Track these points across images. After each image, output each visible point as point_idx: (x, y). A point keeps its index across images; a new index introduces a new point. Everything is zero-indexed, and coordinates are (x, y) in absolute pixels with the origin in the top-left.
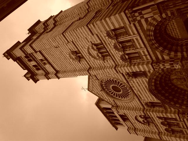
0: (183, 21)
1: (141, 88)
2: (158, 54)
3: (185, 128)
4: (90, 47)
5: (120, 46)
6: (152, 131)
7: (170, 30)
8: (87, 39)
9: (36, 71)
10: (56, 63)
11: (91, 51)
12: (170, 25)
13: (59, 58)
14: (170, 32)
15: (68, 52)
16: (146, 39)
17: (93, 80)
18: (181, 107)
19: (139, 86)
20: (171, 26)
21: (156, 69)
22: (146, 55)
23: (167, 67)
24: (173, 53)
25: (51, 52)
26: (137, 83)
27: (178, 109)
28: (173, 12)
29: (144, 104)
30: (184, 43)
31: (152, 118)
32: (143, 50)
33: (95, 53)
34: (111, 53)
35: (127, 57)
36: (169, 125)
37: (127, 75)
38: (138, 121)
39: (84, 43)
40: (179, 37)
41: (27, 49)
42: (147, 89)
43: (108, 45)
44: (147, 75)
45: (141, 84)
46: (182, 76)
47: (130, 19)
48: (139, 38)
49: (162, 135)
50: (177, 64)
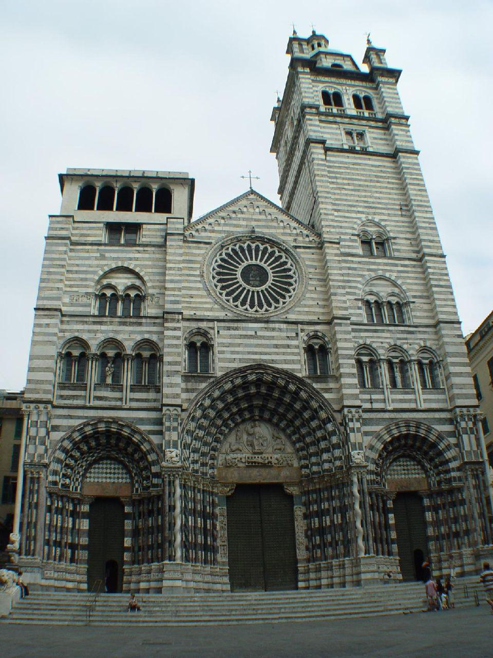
1: (268, 346)
4: (396, 290)
8: (420, 297)
9: (321, 87)
10: (354, 169)
11: (387, 286)
12: (416, 467)
13: (371, 192)
15: (388, 229)
16: (413, 418)
17: (295, 232)
19: (276, 346)
20: (415, 469)
23: (352, 435)
25: (388, 183)
26: (288, 346)
27: (190, 410)
29: (204, 325)
31: (140, 324)
32: (390, 401)
33: (382, 292)
34: (383, 331)
37: (313, 333)
38: (112, 271)
39: (411, 284)
41: (404, 133)
42: (265, 361)
43: (405, 336)
44: (317, 382)
45: (284, 354)
46: (270, 450)
47: (464, 410)
48: (413, 406)
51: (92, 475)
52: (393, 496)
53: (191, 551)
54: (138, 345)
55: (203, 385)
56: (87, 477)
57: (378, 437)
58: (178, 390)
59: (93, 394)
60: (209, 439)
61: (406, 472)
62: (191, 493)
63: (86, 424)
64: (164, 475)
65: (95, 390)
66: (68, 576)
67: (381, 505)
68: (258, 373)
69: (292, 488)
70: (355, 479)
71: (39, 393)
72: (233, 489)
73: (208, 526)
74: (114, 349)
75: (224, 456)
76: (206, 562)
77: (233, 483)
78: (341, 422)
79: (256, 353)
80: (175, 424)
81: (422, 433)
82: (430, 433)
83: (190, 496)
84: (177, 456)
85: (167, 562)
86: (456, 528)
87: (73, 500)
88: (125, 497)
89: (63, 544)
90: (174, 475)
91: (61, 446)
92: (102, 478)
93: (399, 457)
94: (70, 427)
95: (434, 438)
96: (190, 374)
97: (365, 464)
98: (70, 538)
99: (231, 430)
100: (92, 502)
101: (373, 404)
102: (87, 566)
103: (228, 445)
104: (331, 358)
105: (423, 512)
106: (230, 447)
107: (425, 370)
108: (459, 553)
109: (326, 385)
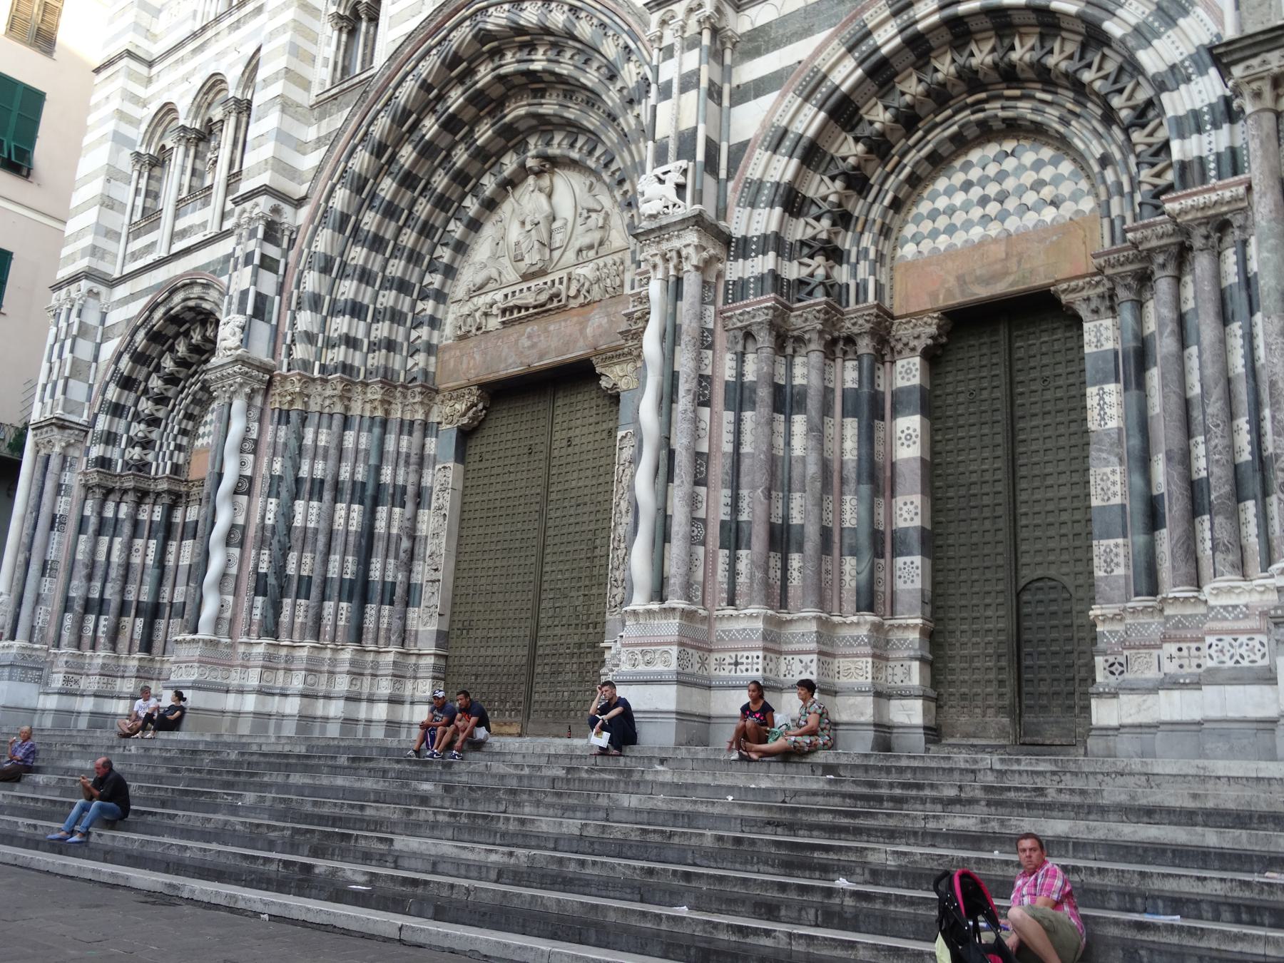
0: (1057, 282)
2: (799, 51)
3: (171, 243)
6: (160, 11)
7: (1001, 177)
12: (1047, 173)
14: (975, 174)
20: (1038, 185)
21: (664, 23)
23: (665, 109)
24: (782, 168)
27: (315, 197)
28: (1204, 178)
30: (854, 275)
36: (203, 136)
40: (917, 239)
46: (570, 256)
49: (131, 75)
50: (680, 188)
57: (812, 85)
63: (153, 307)
68: (475, 14)
69: (617, 369)
70: (655, 289)
71: (74, 261)
73: (381, 526)
87: (158, 494)
93: (961, 143)
96: (326, 95)
99: (475, 225)
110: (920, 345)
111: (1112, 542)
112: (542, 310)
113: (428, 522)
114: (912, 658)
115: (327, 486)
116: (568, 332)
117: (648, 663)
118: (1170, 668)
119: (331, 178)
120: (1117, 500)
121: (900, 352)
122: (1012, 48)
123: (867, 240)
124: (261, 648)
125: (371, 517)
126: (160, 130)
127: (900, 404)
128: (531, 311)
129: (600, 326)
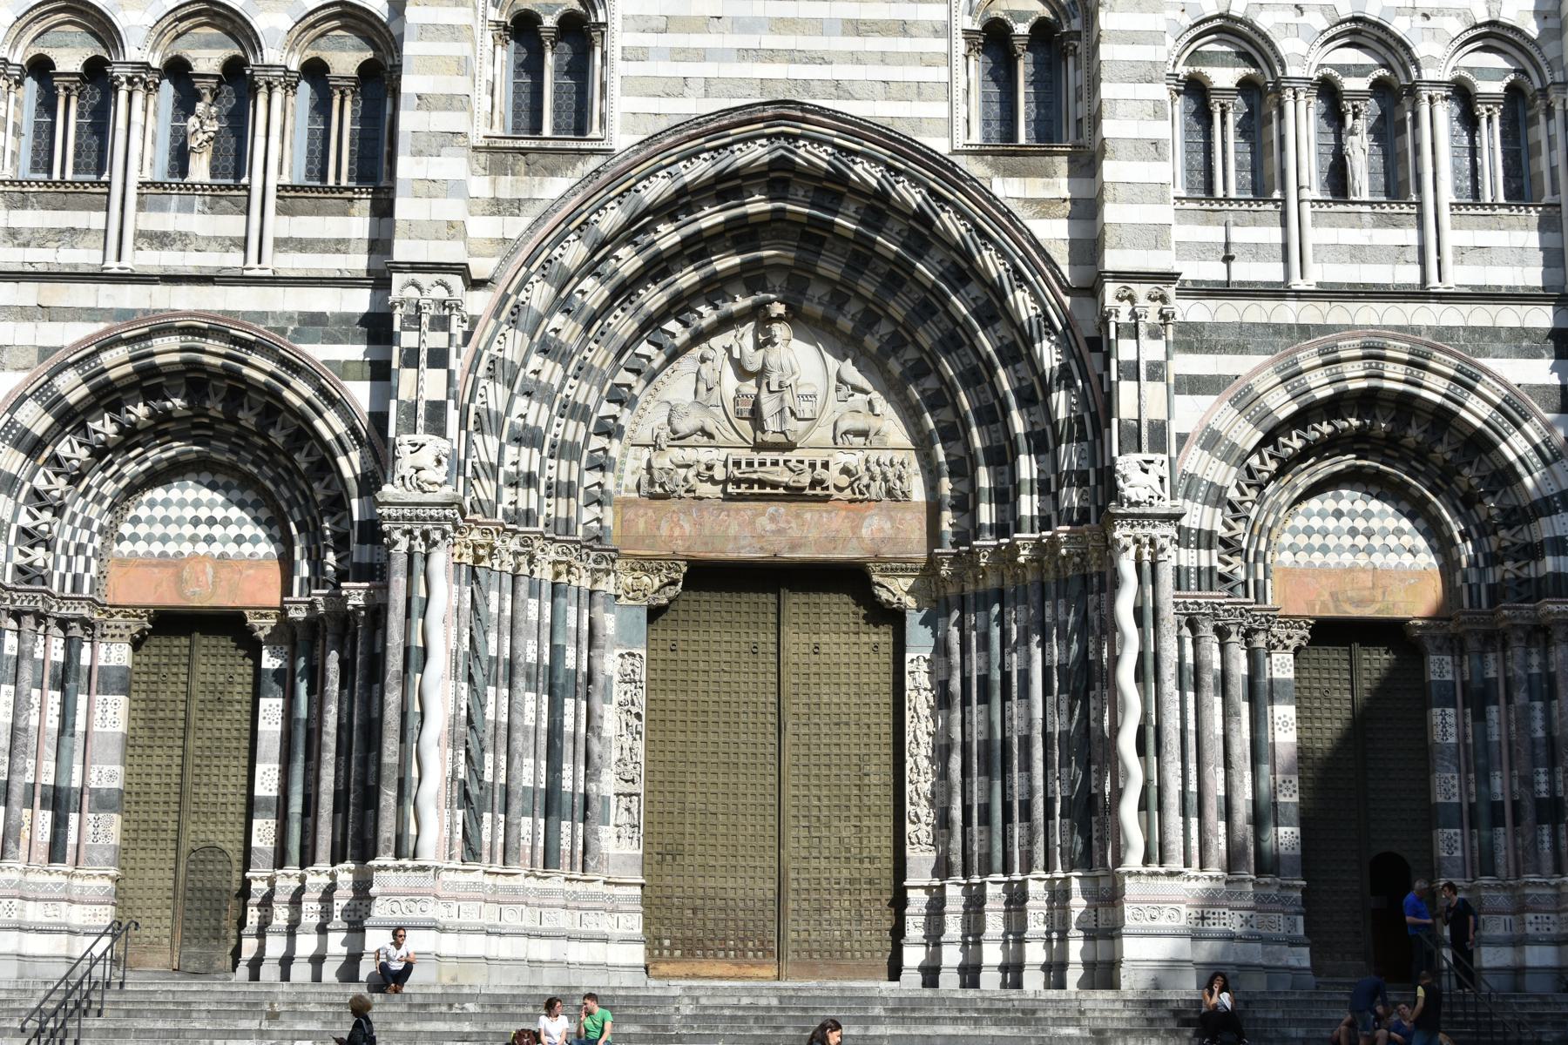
1: (819, 27)
5: (1346, 70)
16: (1398, 328)
18: (514, 323)
19: (857, 28)
22: (1228, 259)
23: (1126, 392)
35: (1224, 77)
45: (884, 58)
48: (1409, 275)
50: (1162, 480)
51: (142, 530)
52: (1299, 635)
53: (487, 816)
54: (313, 26)
55: (554, 187)
56: (121, 539)
57: (1246, 401)
58: (451, 209)
59: (137, 220)
60: (584, 392)
61: (1361, 541)
62: (501, 599)
64: (388, 534)
65: (141, 206)
66: (34, 913)
67: (1240, 667)
68: (778, 136)
72: (674, 583)
73: (568, 722)
74: (224, 46)
75: (646, 454)
76: (550, 859)
77: (673, 559)
78: (1093, 333)
79: (772, 55)
80: (438, 340)
81: (1434, 389)
82: (1471, 389)
83: (494, 609)
84: (439, 462)
85: (386, 859)
86: (1552, 783)
87: (63, 624)
88: (261, 611)
89: (17, 793)
90: (425, 535)
91: (12, 424)
92: (180, 538)
94: (45, 353)
95: (1485, 411)
96: (510, 143)
97: (1165, 506)
98: (49, 766)
99: (674, 355)
100: (141, 632)
101: (1233, 264)
102: (113, 872)
103: (665, 411)
104: (1073, 77)
105: (1426, 706)
106: (670, 422)
107: (1484, 121)
108: (1557, 886)
109: (1046, 186)
110: (1293, 643)
111: (1452, 831)
112: (794, 494)
113: (611, 720)
114: (1297, 913)
115: (520, 670)
116: (834, 526)
117: (1153, 918)
118: (1530, 930)
119: (528, 262)
120: (1456, 800)
121: (1274, 647)
122: (1409, 425)
123: (1262, 548)
124: (476, 876)
125: (556, 710)
126: (36, 29)
127: (1274, 691)
128: (781, 491)
129: (881, 529)
